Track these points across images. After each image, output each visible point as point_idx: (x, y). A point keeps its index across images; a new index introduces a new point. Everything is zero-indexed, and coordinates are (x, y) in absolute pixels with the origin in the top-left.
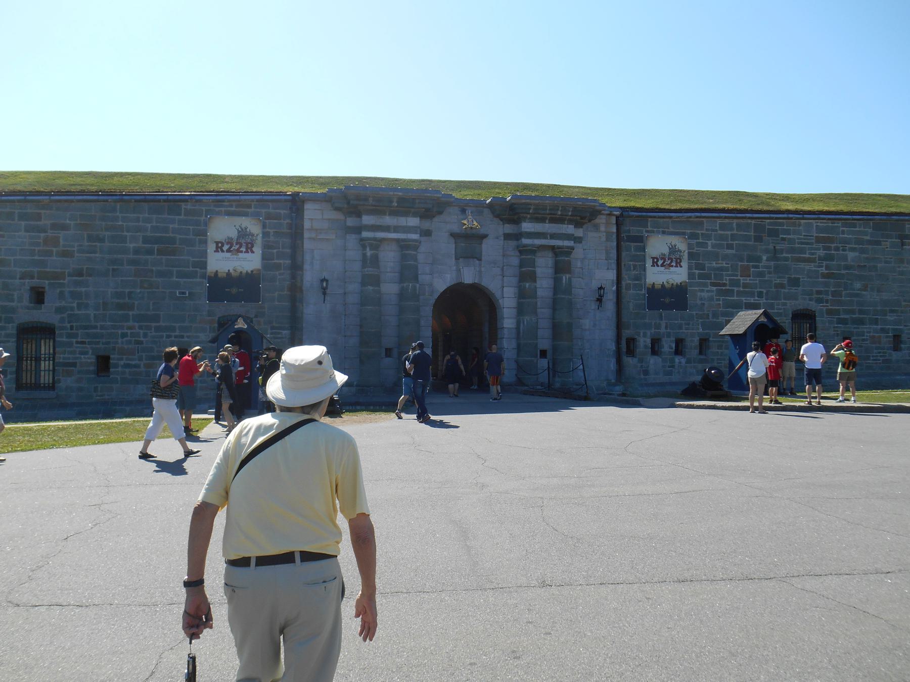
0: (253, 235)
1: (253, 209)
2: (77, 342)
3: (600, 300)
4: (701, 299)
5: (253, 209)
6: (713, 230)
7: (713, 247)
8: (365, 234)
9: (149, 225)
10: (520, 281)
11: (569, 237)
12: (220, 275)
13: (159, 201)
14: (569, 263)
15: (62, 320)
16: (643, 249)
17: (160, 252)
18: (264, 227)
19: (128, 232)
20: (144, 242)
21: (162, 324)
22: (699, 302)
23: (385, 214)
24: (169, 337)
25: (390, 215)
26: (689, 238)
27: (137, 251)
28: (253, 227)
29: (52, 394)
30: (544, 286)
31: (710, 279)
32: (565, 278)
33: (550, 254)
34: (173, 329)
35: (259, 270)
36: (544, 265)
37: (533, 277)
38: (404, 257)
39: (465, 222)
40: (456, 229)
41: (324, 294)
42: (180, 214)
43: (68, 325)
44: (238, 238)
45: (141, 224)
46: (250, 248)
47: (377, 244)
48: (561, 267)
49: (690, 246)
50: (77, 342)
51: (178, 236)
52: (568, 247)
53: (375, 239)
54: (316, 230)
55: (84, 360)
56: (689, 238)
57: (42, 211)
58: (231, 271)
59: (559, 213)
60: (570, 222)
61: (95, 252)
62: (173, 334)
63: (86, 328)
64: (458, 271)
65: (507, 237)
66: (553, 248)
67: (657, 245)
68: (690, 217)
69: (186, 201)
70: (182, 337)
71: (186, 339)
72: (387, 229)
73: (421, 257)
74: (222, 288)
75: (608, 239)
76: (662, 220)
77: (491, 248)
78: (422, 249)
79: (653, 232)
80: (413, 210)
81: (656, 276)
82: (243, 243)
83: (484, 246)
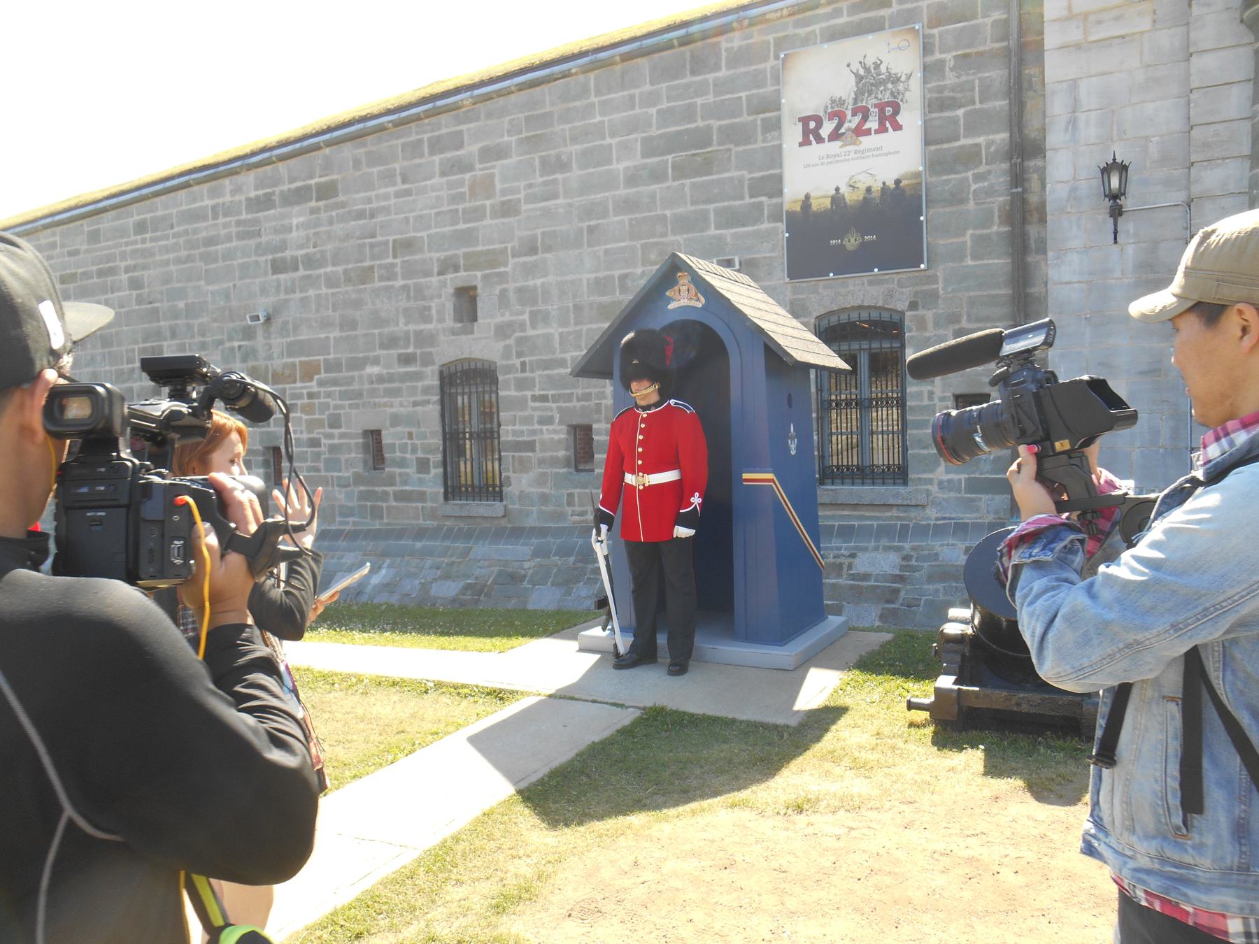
0: (897, 80)
2: (534, 399)
9: (653, 111)
12: (815, 205)
15: (507, 353)
17: (681, 171)
18: (927, 49)
19: (613, 135)
20: (644, 156)
27: (632, 179)
28: (897, 55)
29: (497, 508)
35: (917, 175)
41: (1116, 212)
43: (517, 362)
44: (859, 94)
45: (638, 111)
46: (889, 118)
50: (534, 399)
51: (716, 124)
54: (1085, 16)
55: (546, 436)
57: (464, 127)
58: (844, 190)
61: (555, 196)
63: (548, 365)
82: (873, 107)
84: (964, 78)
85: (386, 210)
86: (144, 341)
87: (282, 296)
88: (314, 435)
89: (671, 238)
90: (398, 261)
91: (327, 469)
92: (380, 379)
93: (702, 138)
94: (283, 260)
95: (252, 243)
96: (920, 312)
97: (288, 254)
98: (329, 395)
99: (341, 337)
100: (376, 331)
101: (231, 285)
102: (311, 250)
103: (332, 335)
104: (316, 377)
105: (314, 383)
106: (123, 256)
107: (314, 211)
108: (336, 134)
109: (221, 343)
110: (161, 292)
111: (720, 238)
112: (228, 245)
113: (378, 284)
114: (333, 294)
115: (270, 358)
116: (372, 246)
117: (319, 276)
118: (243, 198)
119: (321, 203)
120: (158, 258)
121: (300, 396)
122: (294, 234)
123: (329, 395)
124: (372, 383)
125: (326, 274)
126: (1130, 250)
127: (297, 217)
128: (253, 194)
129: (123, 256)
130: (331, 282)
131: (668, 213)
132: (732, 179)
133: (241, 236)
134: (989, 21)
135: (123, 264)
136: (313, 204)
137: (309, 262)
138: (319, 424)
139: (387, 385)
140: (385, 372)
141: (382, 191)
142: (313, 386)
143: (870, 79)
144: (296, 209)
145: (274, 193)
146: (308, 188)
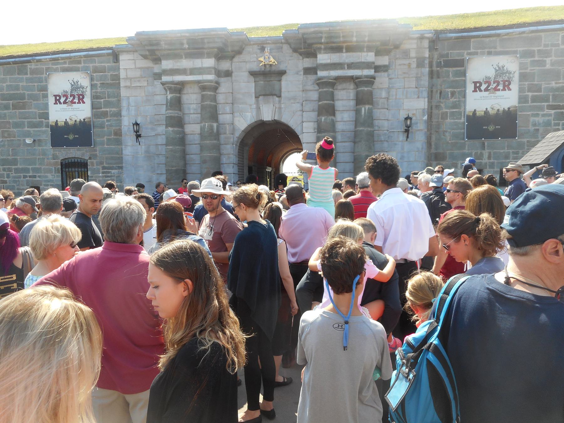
1: (83, 65)
3: (407, 131)
4: (534, 125)
5: (83, 65)
6: (553, 45)
7: (552, 64)
8: (165, 79)
9: (5, 85)
10: (319, 115)
11: (368, 65)
12: (59, 124)
13: (9, 63)
14: (371, 94)
16: (464, 74)
17: (15, 107)
18: (92, 79)
21: (19, 166)
22: (532, 128)
23: (181, 58)
24: (25, 177)
25: (186, 58)
26: (521, 57)
28: (84, 81)
30: (344, 118)
31: (547, 101)
32: (364, 109)
33: (352, 86)
34: (27, 170)
35: (90, 118)
36: (345, 98)
37: (330, 110)
38: (203, 98)
39: (262, 59)
40: (255, 67)
41: (138, 136)
42: (26, 74)
44: (72, 90)
46: (81, 99)
47: (178, 88)
48: (362, 100)
49: (522, 66)
51: (27, 93)
52: (367, 77)
53: (172, 83)
54: (131, 79)
56: (521, 57)
59: (355, 39)
60: (369, 49)
62: (28, 175)
64: (258, 109)
65: (308, 71)
66: (352, 79)
67: (480, 68)
68: (523, 32)
69: (29, 62)
70: (35, 177)
71: (38, 179)
72: (183, 72)
73: (221, 98)
74: (61, 135)
75: (420, 64)
76: (487, 40)
77: (292, 84)
78: (222, 89)
79: (476, 54)
80: (206, 51)
81: (478, 103)
83: (283, 83)
84: (103, 90)
89: (12, 130)
93: (22, 97)
96: (92, 160)
111: (29, 131)
126: (143, 147)
131: (11, 121)
132: (32, 112)
134: (109, 74)
143: (75, 86)
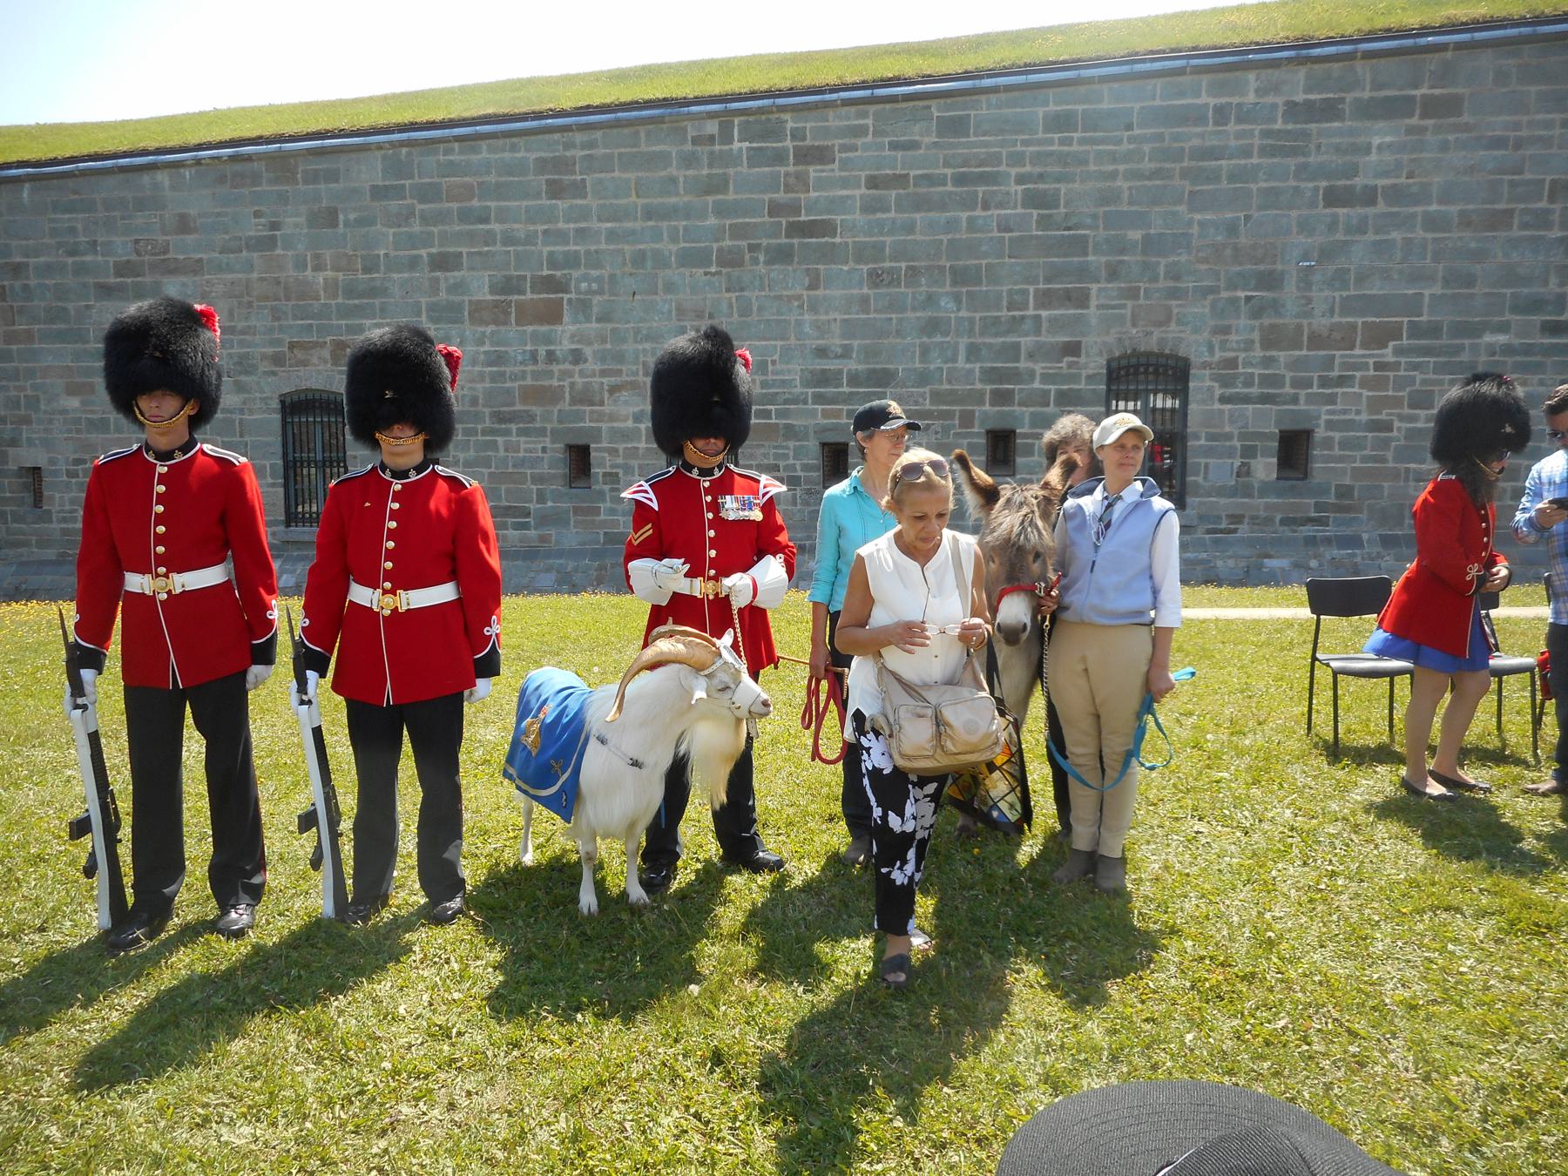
85: (1546, 142)
86: (1048, 280)
87: (1340, 236)
88: (1383, 417)
90: (1557, 206)
91: (1397, 459)
92: (1508, 350)
94: (1352, 187)
95: (1292, 163)
97: (1359, 182)
98: (1415, 366)
99: (1443, 295)
100: (1509, 291)
101: (1242, 215)
102: (1403, 180)
103: (1427, 292)
104: (1391, 344)
105: (1389, 350)
106: (1017, 159)
107: (1411, 130)
108: (1478, 35)
109: (1213, 290)
110: (1095, 217)
112: (1243, 162)
113: (1516, 233)
114: (1435, 240)
115: (1308, 314)
116: (1513, 184)
117: (1414, 215)
118: (1280, 100)
119: (1430, 122)
120: (1092, 168)
121: (1365, 366)
122: (1374, 157)
123: (1415, 366)
124: (1494, 354)
125: (1426, 213)
127: (1382, 135)
128: (1300, 97)
129: (1017, 159)
130: (1432, 223)
133: (1265, 151)
135: (1014, 171)
136: (1414, 121)
137: (1396, 195)
138: (1397, 402)
139: (1519, 359)
140: (1516, 341)
141: (1540, 117)
142: (1388, 354)
144: (1381, 124)
145: (1342, 100)
146: (1412, 99)
